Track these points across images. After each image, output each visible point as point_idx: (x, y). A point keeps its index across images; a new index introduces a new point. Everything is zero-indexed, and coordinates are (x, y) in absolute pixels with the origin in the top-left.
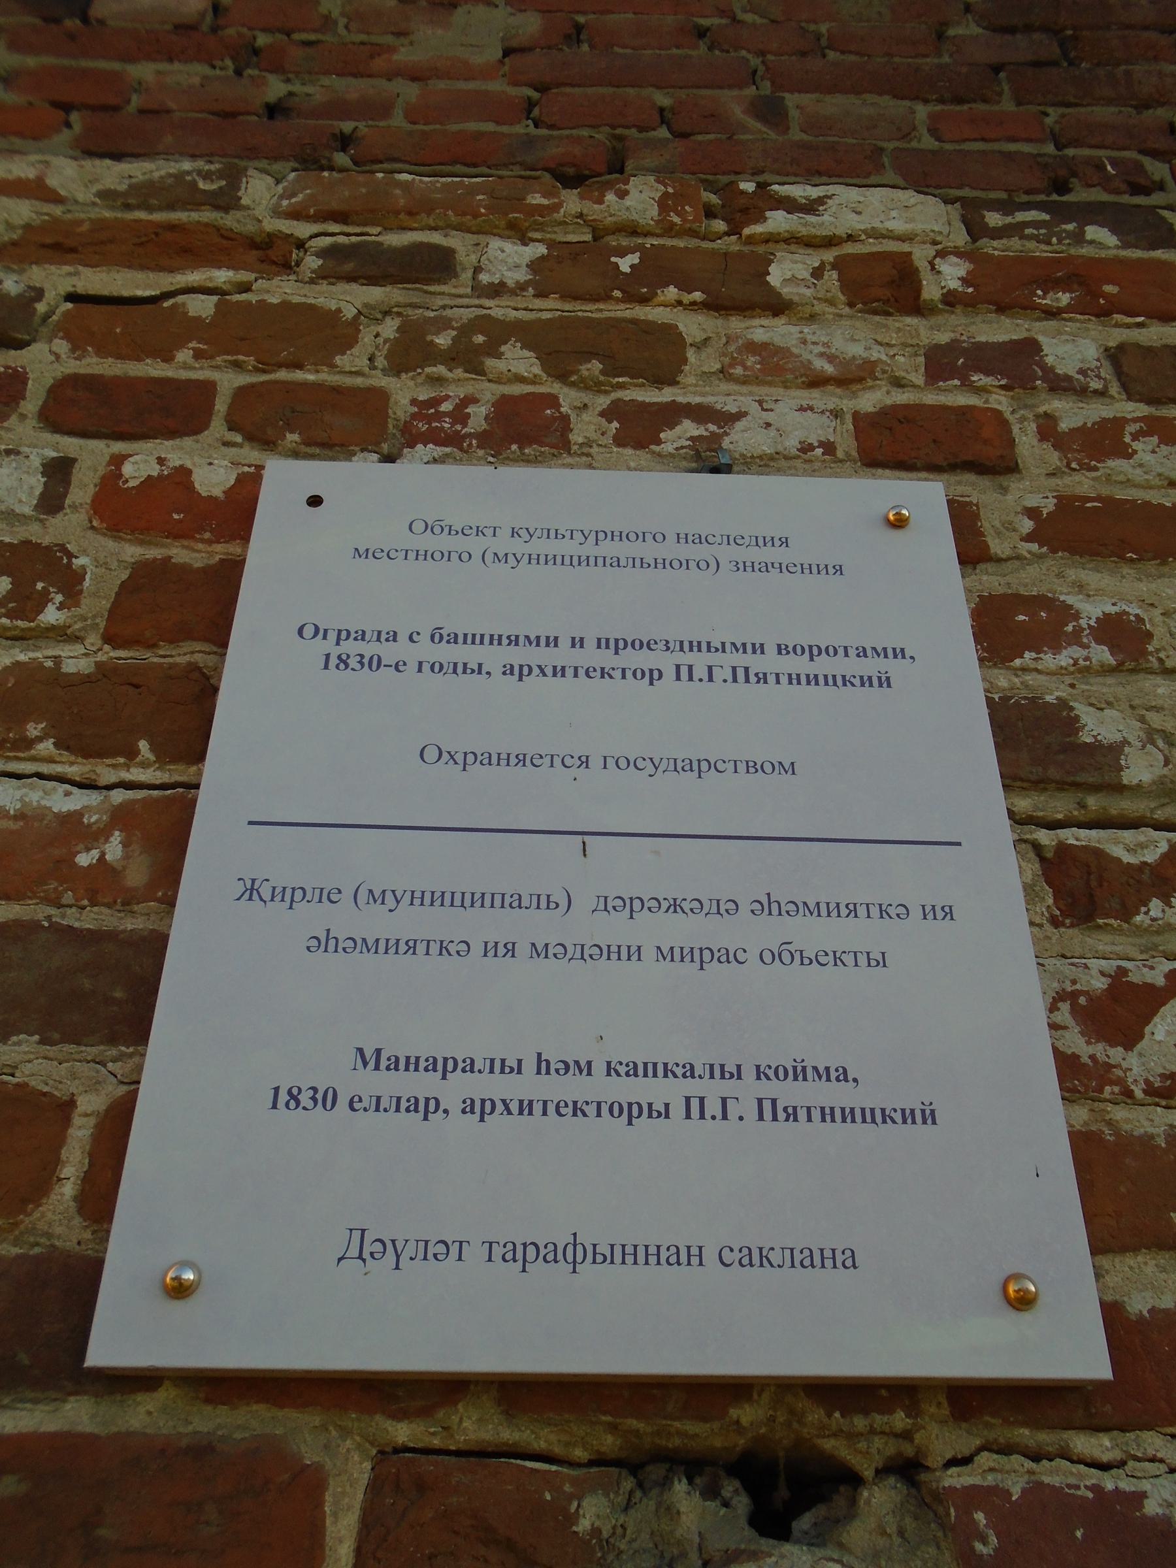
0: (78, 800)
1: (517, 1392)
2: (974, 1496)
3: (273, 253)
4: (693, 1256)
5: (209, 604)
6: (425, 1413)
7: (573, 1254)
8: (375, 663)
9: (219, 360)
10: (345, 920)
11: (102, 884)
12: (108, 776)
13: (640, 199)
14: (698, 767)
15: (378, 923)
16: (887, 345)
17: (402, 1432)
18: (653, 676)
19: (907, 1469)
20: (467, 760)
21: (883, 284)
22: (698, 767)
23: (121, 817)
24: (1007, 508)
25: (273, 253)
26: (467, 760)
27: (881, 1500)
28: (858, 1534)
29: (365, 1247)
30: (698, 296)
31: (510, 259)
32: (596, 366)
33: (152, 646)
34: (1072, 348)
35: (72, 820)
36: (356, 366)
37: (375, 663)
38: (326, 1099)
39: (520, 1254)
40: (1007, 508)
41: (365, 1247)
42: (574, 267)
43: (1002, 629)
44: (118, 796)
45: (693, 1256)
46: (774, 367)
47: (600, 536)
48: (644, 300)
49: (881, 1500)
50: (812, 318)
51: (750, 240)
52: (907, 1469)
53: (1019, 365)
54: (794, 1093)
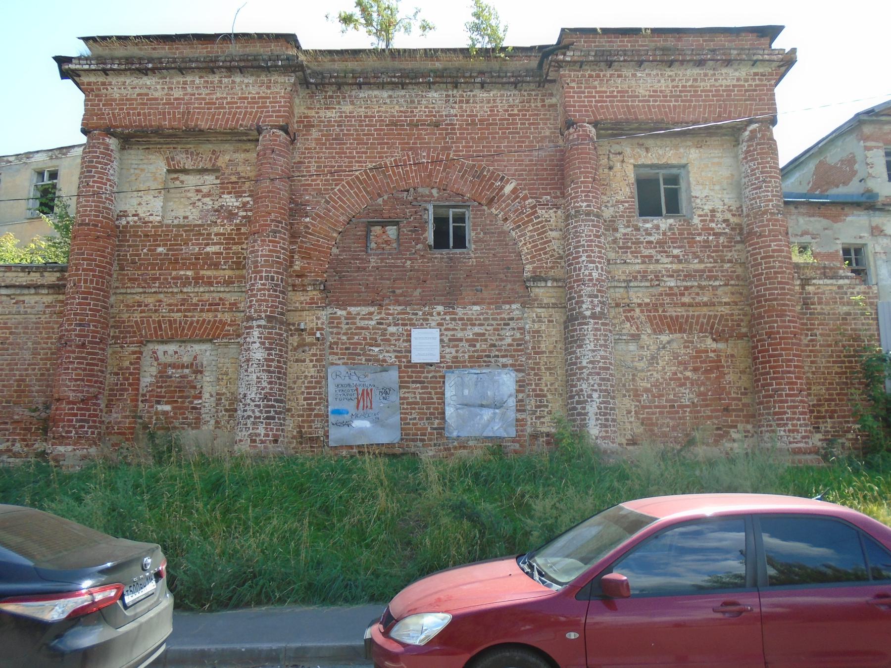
3: (409, 313)
5: (410, 335)
13: (427, 309)
16: (438, 318)
21: (439, 314)
24: (443, 328)
25: (409, 313)
31: (420, 313)
34: (448, 318)
36: (414, 321)
40: (443, 328)
42: (424, 314)
43: (441, 335)
46: (433, 320)
53: (445, 319)
54: (431, 354)
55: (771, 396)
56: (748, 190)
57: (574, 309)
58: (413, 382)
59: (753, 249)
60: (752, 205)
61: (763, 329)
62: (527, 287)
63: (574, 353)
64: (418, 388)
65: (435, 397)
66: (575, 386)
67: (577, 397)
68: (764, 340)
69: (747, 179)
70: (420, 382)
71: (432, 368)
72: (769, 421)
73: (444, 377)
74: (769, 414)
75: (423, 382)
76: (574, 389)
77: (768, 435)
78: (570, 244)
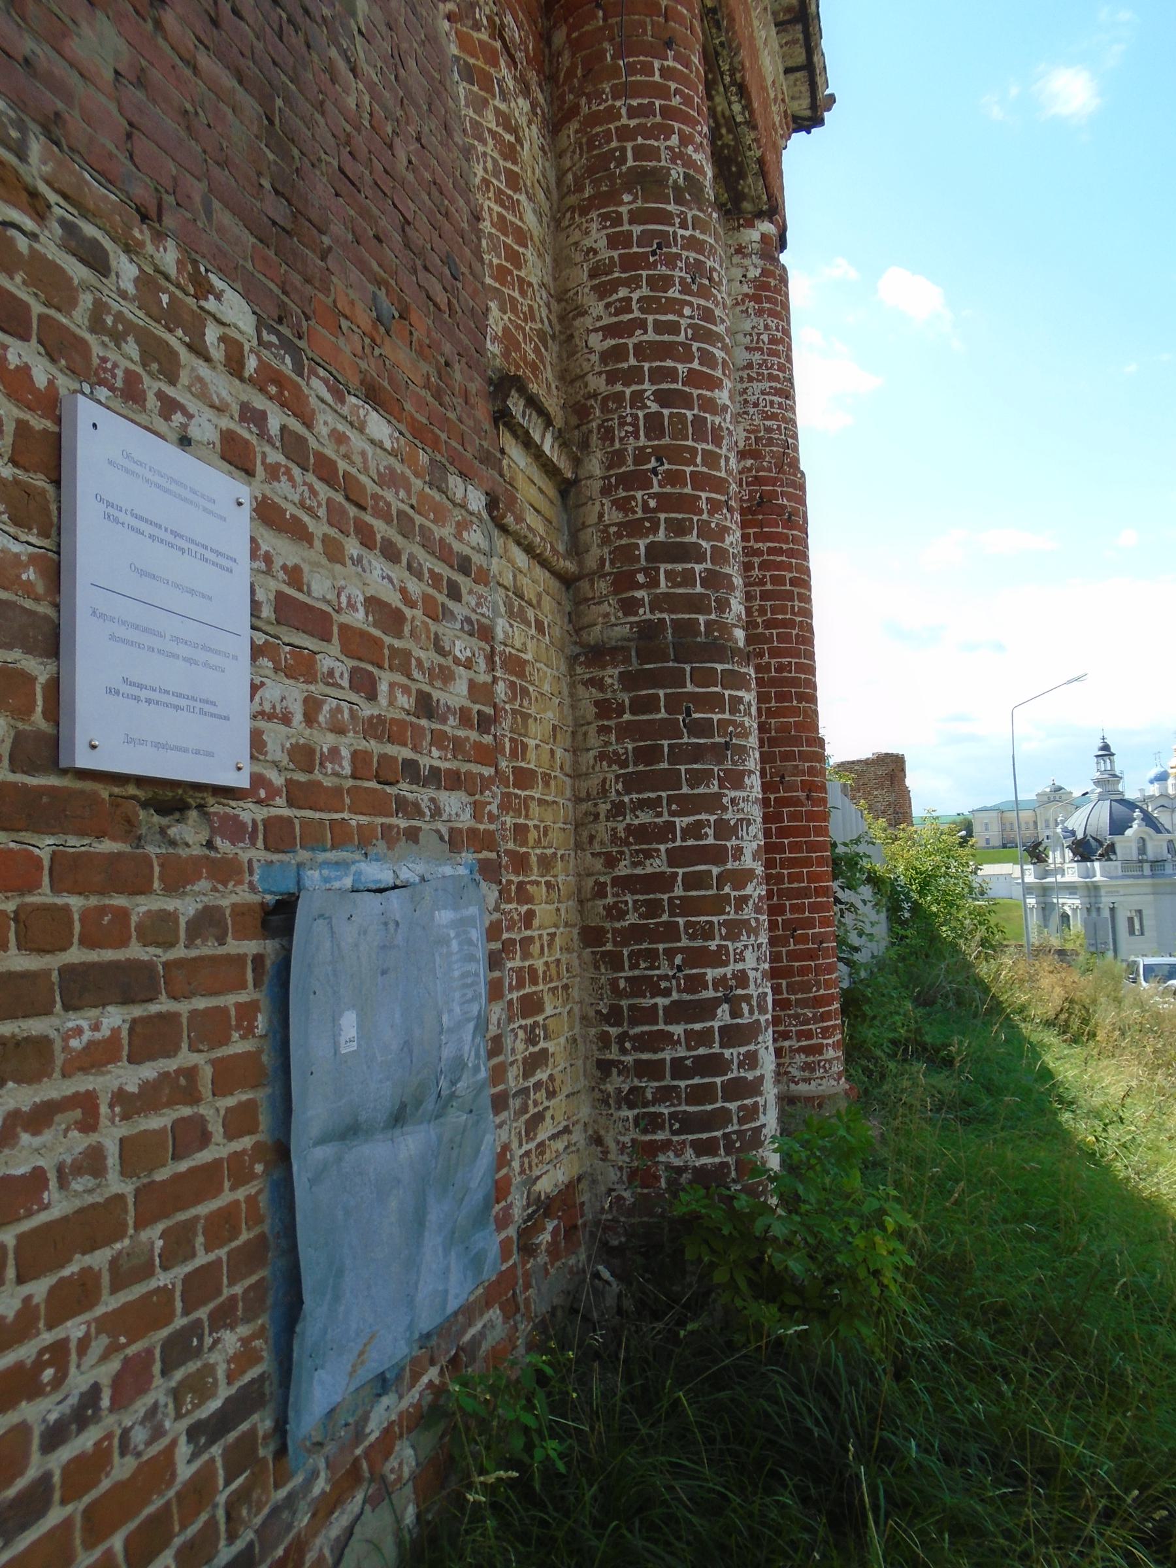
0: (16, 548)
1: (140, 781)
2: (215, 814)
4: (186, 750)
6: (123, 785)
7: (165, 746)
8: (116, 520)
9: (30, 290)
10: (122, 632)
11: (28, 589)
12: (24, 538)
14: (192, 592)
15: (132, 635)
17: (116, 790)
18: (182, 550)
19: (201, 807)
20: (143, 573)
22: (192, 592)
23: (33, 559)
26: (143, 573)
27: (193, 814)
28: (190, 822)
29: (129, 740)
30: (187, 339)
32: (155, 366)
33: (26, 470)
35: (17, 555)
37: (116, 520)
38: (117, 692)
39: (157, 745)
41: (129, 740)
44: (31, 549)
45: (186, 750)
47: (172, 480)
48: (171, 331)
49: (193, 814)
50: (214, 368)
51: (201, 308)
52: (201, 807)
55: (811, 955)
56: (757, 386)
57: (697, 604)
58: (82, 988)
59: (771, 551)
60: (768, 430)
61: (796, 771)
62: (502, 417)
63: (713, 803)
64: (99, 1056)
65: (213, 1110)
66: (717, 959)
67: (723, 1014)
68: (796, 802)
69: (757, 357)
70: (129, 984)
71: (190, 833)
72: (806, 1022)
73: (279, 916)
74: (802, 1003)
75: (129, 984)
76: (711, 974)
77: (801, 1058)
78: (674, 306)
